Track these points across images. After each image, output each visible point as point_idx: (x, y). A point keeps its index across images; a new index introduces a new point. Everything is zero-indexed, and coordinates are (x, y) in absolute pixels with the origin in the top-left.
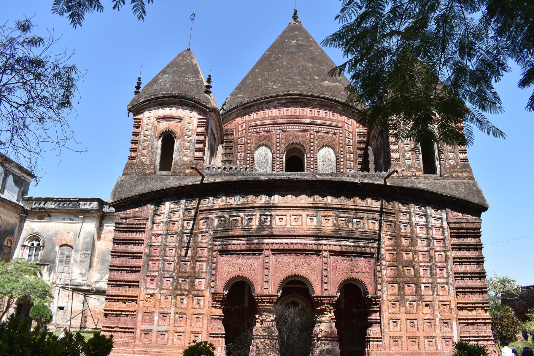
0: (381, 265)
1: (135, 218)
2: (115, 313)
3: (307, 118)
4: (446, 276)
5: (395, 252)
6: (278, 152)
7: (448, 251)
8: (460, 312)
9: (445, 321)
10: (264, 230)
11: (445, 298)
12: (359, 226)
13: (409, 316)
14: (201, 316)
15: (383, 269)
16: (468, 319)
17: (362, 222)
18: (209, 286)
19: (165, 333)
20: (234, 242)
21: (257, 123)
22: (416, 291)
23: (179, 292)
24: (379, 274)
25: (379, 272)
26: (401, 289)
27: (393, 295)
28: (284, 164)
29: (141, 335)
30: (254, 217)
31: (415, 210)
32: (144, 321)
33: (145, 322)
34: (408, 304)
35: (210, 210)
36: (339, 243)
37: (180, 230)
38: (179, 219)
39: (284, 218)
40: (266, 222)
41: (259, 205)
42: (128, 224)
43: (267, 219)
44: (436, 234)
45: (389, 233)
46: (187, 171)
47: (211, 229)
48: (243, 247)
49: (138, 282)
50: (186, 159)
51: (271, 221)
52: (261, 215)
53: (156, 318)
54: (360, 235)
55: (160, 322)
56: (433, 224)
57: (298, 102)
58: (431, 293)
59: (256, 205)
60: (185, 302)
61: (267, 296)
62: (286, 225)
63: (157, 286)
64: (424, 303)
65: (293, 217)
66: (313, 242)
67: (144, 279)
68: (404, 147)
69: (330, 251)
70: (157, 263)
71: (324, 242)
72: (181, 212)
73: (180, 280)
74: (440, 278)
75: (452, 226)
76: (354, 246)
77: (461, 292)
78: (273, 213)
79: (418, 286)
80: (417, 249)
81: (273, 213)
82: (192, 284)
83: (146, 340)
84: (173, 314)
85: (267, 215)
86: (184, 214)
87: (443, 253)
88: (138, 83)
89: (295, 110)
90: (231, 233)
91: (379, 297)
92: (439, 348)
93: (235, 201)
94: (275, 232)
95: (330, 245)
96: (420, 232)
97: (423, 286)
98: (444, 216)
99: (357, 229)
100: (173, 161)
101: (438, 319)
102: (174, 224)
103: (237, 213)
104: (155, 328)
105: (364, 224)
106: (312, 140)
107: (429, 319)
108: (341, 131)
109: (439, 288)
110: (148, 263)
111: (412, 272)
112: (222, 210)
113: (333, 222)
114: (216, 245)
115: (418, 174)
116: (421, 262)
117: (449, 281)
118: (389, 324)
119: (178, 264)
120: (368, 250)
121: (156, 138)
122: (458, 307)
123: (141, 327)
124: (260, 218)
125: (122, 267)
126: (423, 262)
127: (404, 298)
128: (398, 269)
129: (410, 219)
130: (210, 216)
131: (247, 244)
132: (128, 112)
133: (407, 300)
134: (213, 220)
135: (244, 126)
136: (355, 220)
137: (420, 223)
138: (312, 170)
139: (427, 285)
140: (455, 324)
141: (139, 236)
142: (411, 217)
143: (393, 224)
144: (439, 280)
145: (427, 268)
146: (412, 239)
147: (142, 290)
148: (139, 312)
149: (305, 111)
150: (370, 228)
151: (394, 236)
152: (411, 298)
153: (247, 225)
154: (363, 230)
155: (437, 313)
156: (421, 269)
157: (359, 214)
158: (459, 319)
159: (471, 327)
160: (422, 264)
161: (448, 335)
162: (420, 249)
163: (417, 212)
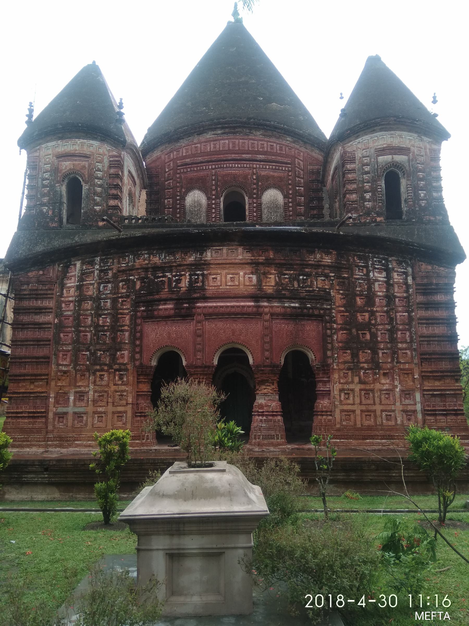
0: (331, 328)
1: (39, 282)
2: (21, 395)
3: (248, 154)
4: (409, 341)
5: (348, 314)
6: (214, 197)
7: (412, 311)
8: (426, 383)
9: (406, 392)
10: (195, 293)
11: (407, 366)
12: (306, 284)
13: (363, 386)
14: (125, 394)
15: (334, 333)
16: (435, 390)
17: (309, 280)
18: (132, 359)
19: (83, 415)
20: (161, 307)
21: (188, 160)
22: (372, 358)
23: (98, 367)
24: (329, 340)
25: (329, 336)
26: (355, 355)
27: (345, 362)
28: (222, 213)
29: (54, 419)
30: (183, 278)
31: (373, 264)
32: (57, 402)
33: (58, 404)
34: (362, 373)
35: (130, 270)
36: (283, 305)
37: (95, 295)
38: (94, 282)
39: (219, 278)
40: (198, 283)
41: (188, 262)
42: (30, 290)
43: (198, 278)
44: (398, 292)
45: (341, 292)
46: (101, 224)
47: (133, 292)
48: (172, 312)
49: (49, 358)
50: (97, 208)
51: (203, 282)
52: (190, 275)
53: (72, 398)
54: (306, 295)
55: (77, 403)
56: (395, 280)
57: (237, 132)
58: (389, 360)
59: (185, 263)
60: (106, 378)
61: (201, 367)
62: (221, 285)
63: (71, 361)
64: (382, 372)
65: (229, 276)
66: (252, 304)
67: (55, 354)
68: (363, 187)
69: (272, 315)
70: (70, 335)
71: (266, 304)
72: (96, 274)
73: (99, 353)
74: (401, 342)
75: (419, 280)
76: (299, 308)
77: (426, 359)
78: (205, 272)
79: (375, 352)
80: (375, 309)
81: (205, 272)
82: (113, 358)
83: (61, 424)
84: (91, 393)
85: (198, 275)
86: (99, 276)
87: (406, 314)
88: (29, 109)
89: (234, 143)
90: (157, 297)
91: (328, 365)
92: (399, 422)
93: (160, 258)
94: (208, 293)
95: (272, 307)
96: (379, 290)
97: (380, 353)
98: (410, 269)
99: (303, 287)
100: (82, 211)
101: (398, 390)
102: (88, 288)
103: (163, 273)
104: (70, 409)
105: (311, 282)
106: (255, 181)
107: (386, 390)
108: (290, 169)
109: (400, 355)
110: (59, 336)
111: (368, 337)
112: (146, 269)
113: (276, 280)
114: (139, 311)
115: (378, 219)
116: (379, 325)
117: (412, 346)
118: (340, 396)
119: (95, 335)
120: (316, 312)
121: (58, 182)
122: (423, 376)
123: (52, 410)
124: (190, 279)
125: (27, 341)
126: (382, 324)
127: (358, 366)
128: (350, 333)
129: (367, 274)
130: (131, 278)
131: (176, 309)
132: (19, 148)
133: (362, 368)
134: (135, 283)
135: (172, 165)
136: (301, 277)
137: (379, 279)
138: (255, 218)
139: (385, 351)
140: (418, 396)
141: (46, 303)
142: (368, 272)
143: (346, 281)
144: (400, 345)
145: (386, 332)
146: (370, 298)
147: (53, 366)
148: (51, 392)
149: (246, 144)
150: (319, 286)
151: (347, 295)
152: (366, 366)
153: (175, 287)
154: (311, 289)
155: (396, 383)
156: (379, 333)
157: (307, 270)
158: (424, 390)
159: (438, 399)
160: (380, 327)
161: (410, 408)
162: (378, 309)
163: (376, 266)
